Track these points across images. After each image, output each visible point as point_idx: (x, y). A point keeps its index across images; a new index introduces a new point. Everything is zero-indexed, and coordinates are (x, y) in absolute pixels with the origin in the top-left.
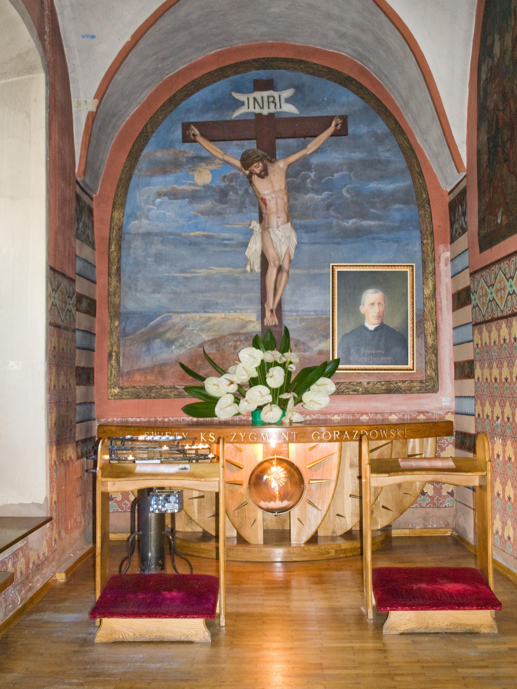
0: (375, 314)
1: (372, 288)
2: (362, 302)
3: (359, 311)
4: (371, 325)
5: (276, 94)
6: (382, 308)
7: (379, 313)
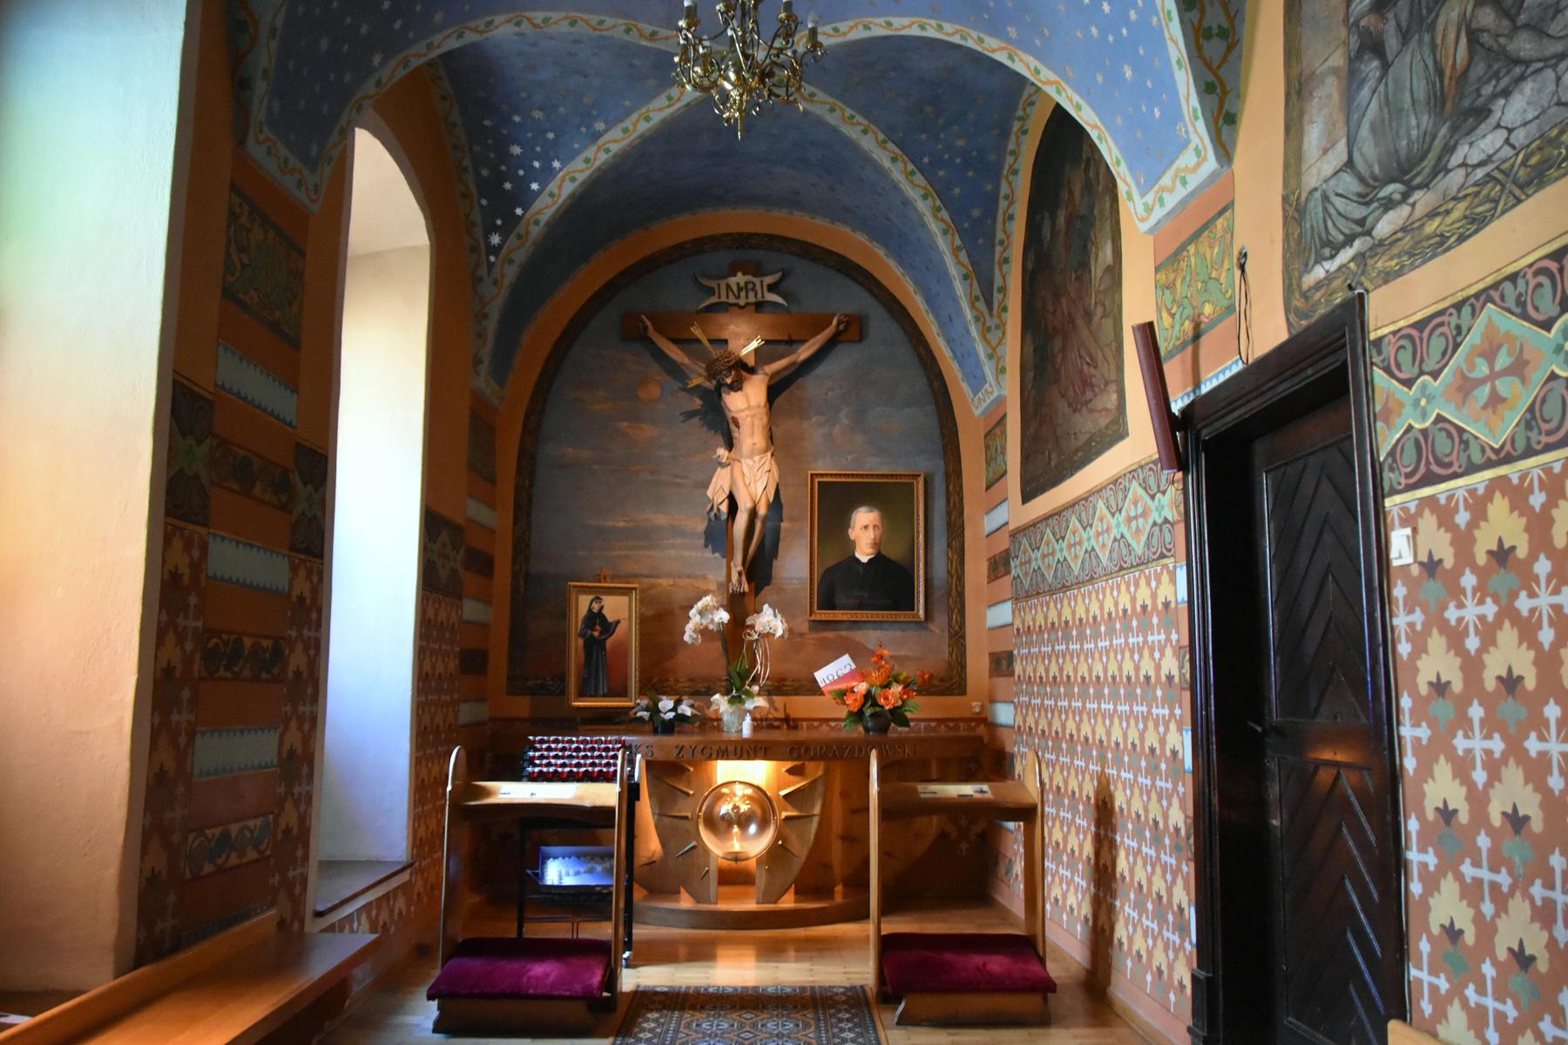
4: (864, 555)
5: (757, 281)
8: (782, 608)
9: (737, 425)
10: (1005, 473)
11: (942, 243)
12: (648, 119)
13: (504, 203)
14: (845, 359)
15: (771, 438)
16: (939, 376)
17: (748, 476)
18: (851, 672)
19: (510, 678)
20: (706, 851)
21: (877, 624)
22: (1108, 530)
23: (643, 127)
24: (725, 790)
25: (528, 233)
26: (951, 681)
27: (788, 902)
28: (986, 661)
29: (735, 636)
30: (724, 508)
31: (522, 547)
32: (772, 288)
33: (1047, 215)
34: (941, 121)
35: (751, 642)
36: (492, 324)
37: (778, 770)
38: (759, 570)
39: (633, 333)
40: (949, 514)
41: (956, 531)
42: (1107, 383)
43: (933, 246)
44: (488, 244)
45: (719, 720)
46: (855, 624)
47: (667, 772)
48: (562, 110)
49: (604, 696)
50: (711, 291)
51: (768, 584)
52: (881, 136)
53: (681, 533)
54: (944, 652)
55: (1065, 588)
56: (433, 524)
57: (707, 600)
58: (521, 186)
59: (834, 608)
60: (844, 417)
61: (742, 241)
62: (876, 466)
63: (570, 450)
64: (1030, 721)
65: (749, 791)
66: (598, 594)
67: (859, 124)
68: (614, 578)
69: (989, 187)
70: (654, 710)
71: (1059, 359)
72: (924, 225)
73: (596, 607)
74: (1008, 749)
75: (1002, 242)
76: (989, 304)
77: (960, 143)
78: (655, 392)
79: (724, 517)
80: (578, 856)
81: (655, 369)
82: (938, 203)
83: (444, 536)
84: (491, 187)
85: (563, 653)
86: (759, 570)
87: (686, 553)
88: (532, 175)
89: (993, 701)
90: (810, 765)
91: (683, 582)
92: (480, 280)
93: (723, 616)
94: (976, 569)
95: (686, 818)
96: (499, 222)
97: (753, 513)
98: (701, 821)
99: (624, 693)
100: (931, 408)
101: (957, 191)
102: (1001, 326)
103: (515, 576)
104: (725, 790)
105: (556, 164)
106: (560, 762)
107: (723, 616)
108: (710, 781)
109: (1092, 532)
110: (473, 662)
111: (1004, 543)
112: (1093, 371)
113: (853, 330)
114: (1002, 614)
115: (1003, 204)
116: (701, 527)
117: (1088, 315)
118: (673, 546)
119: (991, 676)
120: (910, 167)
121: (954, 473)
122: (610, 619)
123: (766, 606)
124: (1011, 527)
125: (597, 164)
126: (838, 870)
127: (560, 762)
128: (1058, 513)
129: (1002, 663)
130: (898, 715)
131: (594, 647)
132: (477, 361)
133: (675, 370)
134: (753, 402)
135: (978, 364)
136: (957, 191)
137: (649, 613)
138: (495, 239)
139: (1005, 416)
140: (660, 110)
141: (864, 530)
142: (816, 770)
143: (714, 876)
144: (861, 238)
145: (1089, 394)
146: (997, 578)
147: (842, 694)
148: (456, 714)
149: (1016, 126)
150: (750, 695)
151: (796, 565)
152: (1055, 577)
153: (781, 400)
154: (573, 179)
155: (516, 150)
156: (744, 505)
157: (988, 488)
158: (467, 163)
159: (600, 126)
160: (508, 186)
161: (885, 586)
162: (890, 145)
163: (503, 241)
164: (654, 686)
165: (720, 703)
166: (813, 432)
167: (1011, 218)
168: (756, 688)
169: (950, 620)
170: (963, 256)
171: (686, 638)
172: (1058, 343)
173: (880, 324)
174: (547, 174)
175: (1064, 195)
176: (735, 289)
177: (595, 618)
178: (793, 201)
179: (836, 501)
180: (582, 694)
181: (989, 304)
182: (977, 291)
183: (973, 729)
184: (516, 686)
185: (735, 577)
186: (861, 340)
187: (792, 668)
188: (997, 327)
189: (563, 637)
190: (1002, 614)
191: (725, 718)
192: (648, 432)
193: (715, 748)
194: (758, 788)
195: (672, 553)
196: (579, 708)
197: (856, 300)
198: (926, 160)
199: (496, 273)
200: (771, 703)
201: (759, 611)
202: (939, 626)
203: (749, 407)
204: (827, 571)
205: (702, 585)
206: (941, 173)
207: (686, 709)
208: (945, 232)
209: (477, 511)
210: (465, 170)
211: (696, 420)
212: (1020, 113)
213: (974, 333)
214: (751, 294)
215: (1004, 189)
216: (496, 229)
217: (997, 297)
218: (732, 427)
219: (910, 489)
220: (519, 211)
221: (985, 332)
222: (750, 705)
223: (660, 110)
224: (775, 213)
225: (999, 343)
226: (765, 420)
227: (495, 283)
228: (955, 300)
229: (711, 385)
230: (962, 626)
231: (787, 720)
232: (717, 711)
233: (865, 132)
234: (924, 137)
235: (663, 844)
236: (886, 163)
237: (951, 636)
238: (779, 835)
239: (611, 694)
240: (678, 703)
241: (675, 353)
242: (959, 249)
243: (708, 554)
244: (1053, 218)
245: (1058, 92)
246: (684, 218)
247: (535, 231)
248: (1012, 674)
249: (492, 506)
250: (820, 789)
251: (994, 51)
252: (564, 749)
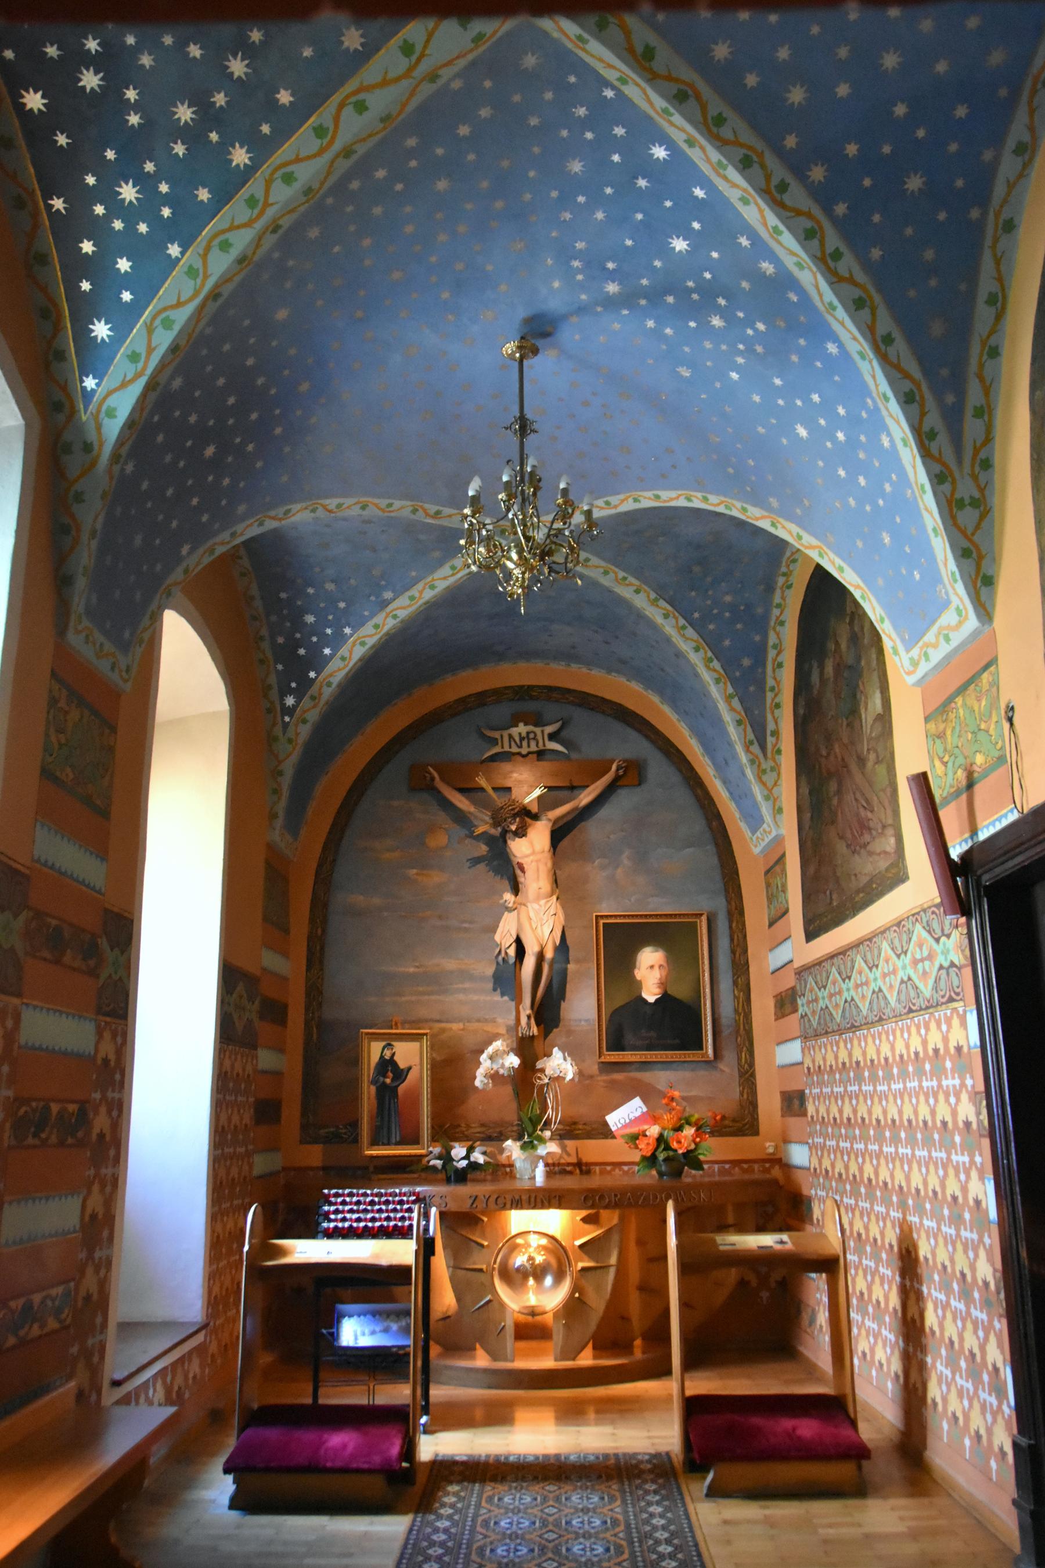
0: (656, 981)
2: (638, 964)
3: (634, 977)
4: (651, 996)
5: (538, 730)
6: (664, 974)
8: (572, 1051)
9: (523, 870)
10: (786, 911)
11: (714, 691)
12: (432, 587)
13: (298, 666)
14: (625, 800)
15: (556, 882)
16: (718, 816)
17: (535, 919)
18: (643, 1114)
19: (304, 1127)
20: (502, 1305)
21: (666, 1065)
22: (894, 972)
23: (428, 595)
24: (519, 1241)
25: (320, 694)
26: (742, 1122)
27: (586, 1359)
28: (777, 1102)
29: (525, 1080)
30: (512, 952)
31: (315, 993)
32: (552, 737)
33: (815, 665)
34: (709, 579)
35: (542, 1086)
36: (286, 781)
37: (573, 1219)
38: (548, 1012)
39: (421, 784)
40: (733, 952)
41: (741, 968)
42: (884, 827)
43: (706, 694)
44: (283, 705)
45: (511, 1166)
46: (645, 1065)
47: (462, 1223)
48: (352, 582)
49: (398, 1143)
50: (494, 742)
51: (557, 1026)
52: (653, 595)
53: (471, 978)
54: (735, 1092)
55: (854, 1028)
56: (232, 977)
57: (498, 1045)
58: (315, 652)
59: (623, 1050)
60: (625, 860)
61: (523, 693)
62: (660, 906)
63: (362, 898)
64: (826, 1163)
65: (544, 1241)
66: (389, 1040)
67: (630, 584)
68: (404, 1023)
69: (757, 638)
70: (447, 1158)
71: (835, 801)
72: (697, 675)
73: (388, 1054)
74: (805, 1192)
75: (772, 689)
76: (763, 747)
77: (728, 598)
78: (440, 839)
79: (512, 960)
80: (374, 1314)
81: (441, 817)
82: (710, 654)
83: (240, 988)
84: (287, 654)
85: (355, 1099)
86: (548, 1012)
87: (476, 998)
88: (325, 641)
89: (786, 1141)
90: (604, 1214)
91: (475, 1025)
92: (276, 739)
93: (513, 1061)
94: (762, 1006)
95: (481, 1270)
96: (293, 685)
97: (540, 957)
98: (496, 1274)
99: (416, 1141)
100: (711, 848)
101: (727, 643)
102: (776, 769)
103: (307, 1023)
104: (519, 1241)
105: (347, 630)
106: (355, 1216)
107: (513, 1061)
108: (504, 1229)
109: (878, 973)
110: (267, 1111)
111: (789, 981)
112: (869, 815)
113: (632, 774)
114: (791, 1052)
115: (771, 653)
116: (490, 971)
117: (862, 761)
118: (465, 991)
119: (783, 1116)
120: (682, 622)
121: (736, 912)
122: (402, 1065)
123: (556, 1050)
124: (797, 964)
125: (386, 629)
126: (637, 1324)
127: (355, 1216)
128: (842, 953)
129: (794, 1102)
130: (691, 1158)
131: (386, 1094)
132: (273, 816)
133: (461, 819)
134: (538, 847)
135: (756, 805)
136: (727, 643)
137: (438, 1058)
138: (290, 701)
139: (783, 855)
140: (445, 578)
142: (611, 1218)
143: (510, 1331)
144: (636, 686)
145: (867, 837)
146: (784, 1016)
147: (634, 1139)
148: (251, 1166)
149: (781, 580)
150: (542, 1140)
151: (583, 1007)
152: (843, 1016)
153: (565, 843)
154: (363, 644)
155: (310, 619)
156: (531, 950)
157: (771, 925)
158: (264, 632)
159: (388, 595)
160: (302, 651)
161: (674, 1025)
162: (662, 603)
163: (298, 702)
164: (447, 1131)
165: (512, 1149)
166: (597, 875)
167: (780, 665)
168: (547, 1134)
169: (739, 1059)
170: (736, 703)
171: (478, 1083)
172: (833, 786)
173: (658, 768)
174: (338, 640)
175: (832, 646)
176: (517, 739)
177: (387, 1065)
178: (569, 655)
179: (621, 941)
180: (374, 1143)
181: (763, 747)
182: (751, 736)
183: (767, 1171)
184: (309, 1134)
185: (524, 1020)
186: (639, 784)
187: (583, 1111)
188: (772, 769)
189: (353, 1085)
190: (791, 1052)
191: (518, 1165)
192: (436, 878)
193: (509, 1197)
194: (553, 1238)
195: (461, 997)
196: (372, 1157)
197: (636, 746)
198: (696, 615)
199: (291, 732)
200: (564, 1148)
201: (549, 1055)
202: (728, 1066)
203: (533, 853)
205: (489, 1028)
206: (711, 627)
207: (478, 1157)
208: (717, 681)
209: (271, 960)
210: (262, 638)
211: (482, 867)
212: (784, 569)
213: (749, 773)
214: (533, 744)
215: (772, 639)
216: (291, 691)
217: (770, 740)
218: (518, 872)
219: (692, 929)
220: (312, 675)
221: (760, 773)
222: (542, 1151)
223: (445, 578)
224: (554, 665)
225: (775, 784)
226: (550, 864)
227: (290, 741)
228: (730, 744)
229: (496, 832)
230: (752, 1065)
231: (579, 1164)
232: (509, 1157)
233: (637, 592)
234: (693, 593)
235: (459, 1299)
236: (659, 620)
237: (741, 1075)
238: (576, 1288)
239: (402, 1142)
240: (470, 1150)
241: (461, 802)
242: (731, 696)
243: (497, 997)
244: (822, 667)
245: (821, 555)
246: (466, 674)
247: (327, 693)
248: (804, 1113)
249: (285, 954)
250: (616, 1238)
251: (757, 519)
252: (358, 1203)
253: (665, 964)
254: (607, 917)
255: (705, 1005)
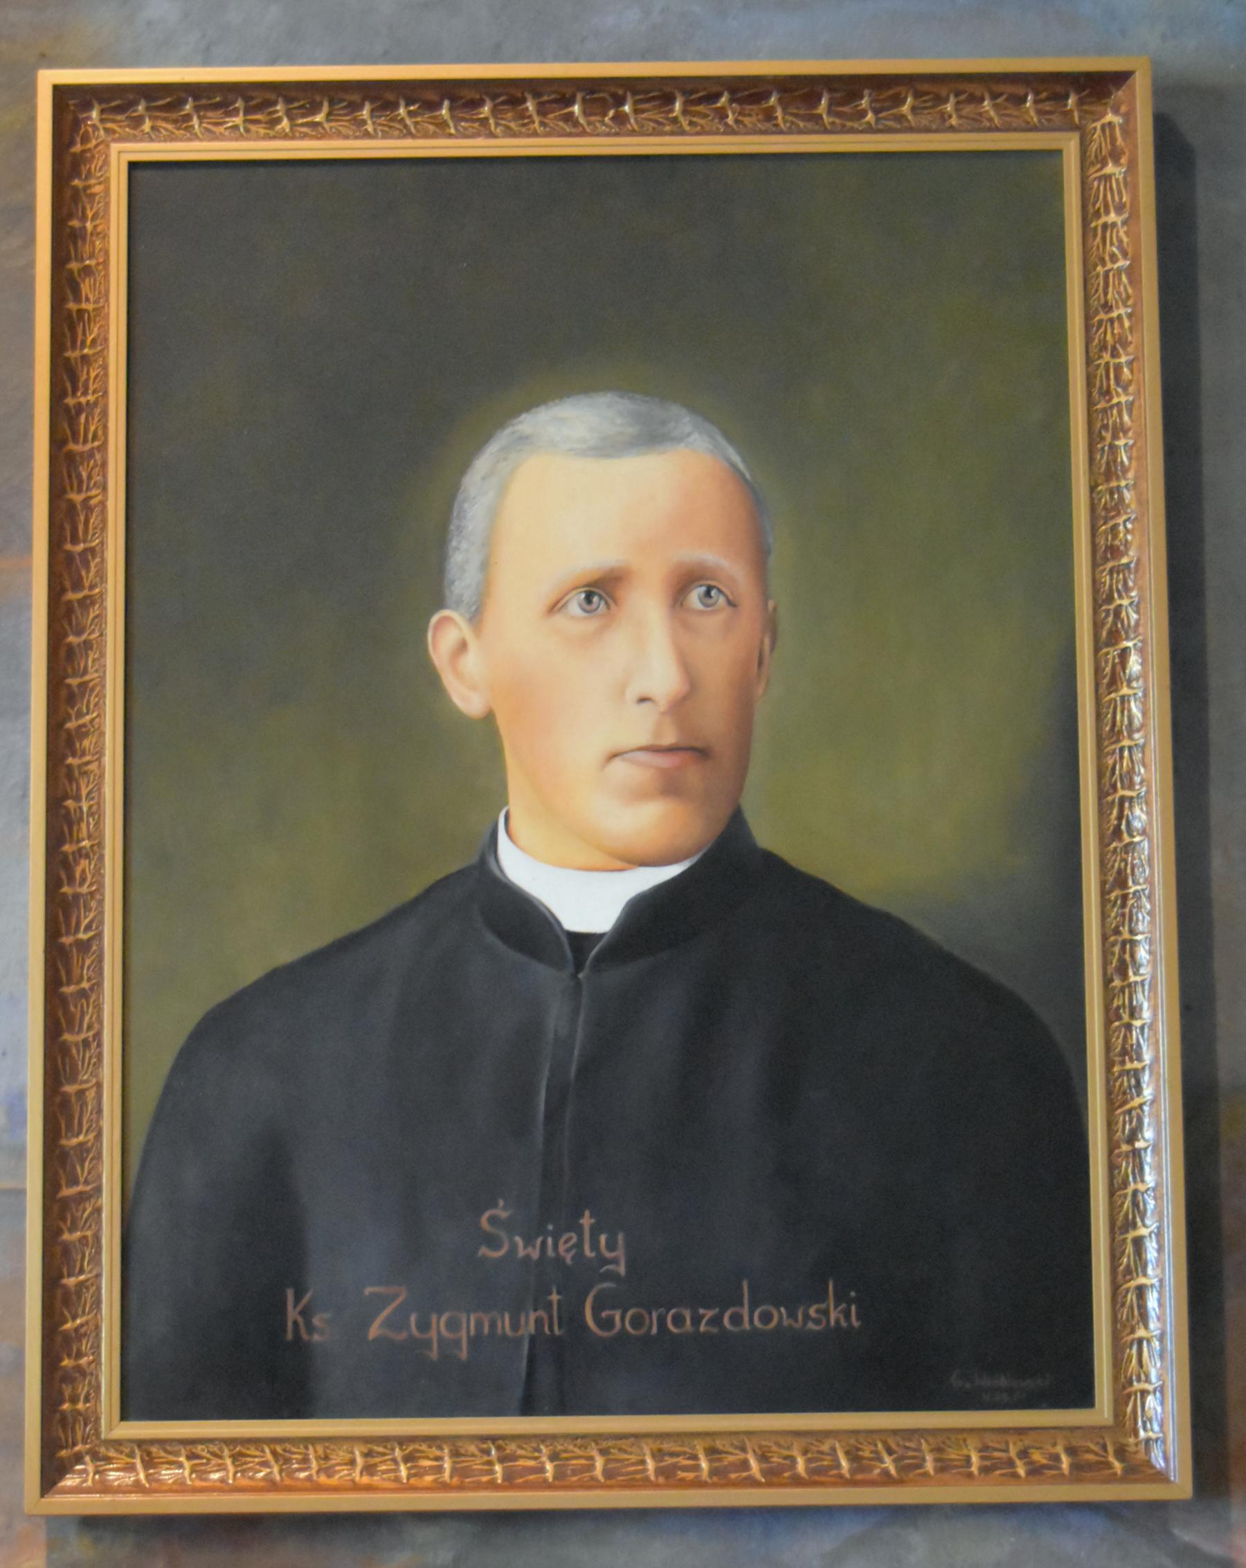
0: (639, 728)
1: (587, 387)
2: (463, 561)
6: (721, 644)
7: (681, 707)
59: (293, 1399)
141: (588, 633)
204: (222, 1028)
219: (1014, 214)
253: (733, 569)
254: (168, 101)
255: (1120, 965)
